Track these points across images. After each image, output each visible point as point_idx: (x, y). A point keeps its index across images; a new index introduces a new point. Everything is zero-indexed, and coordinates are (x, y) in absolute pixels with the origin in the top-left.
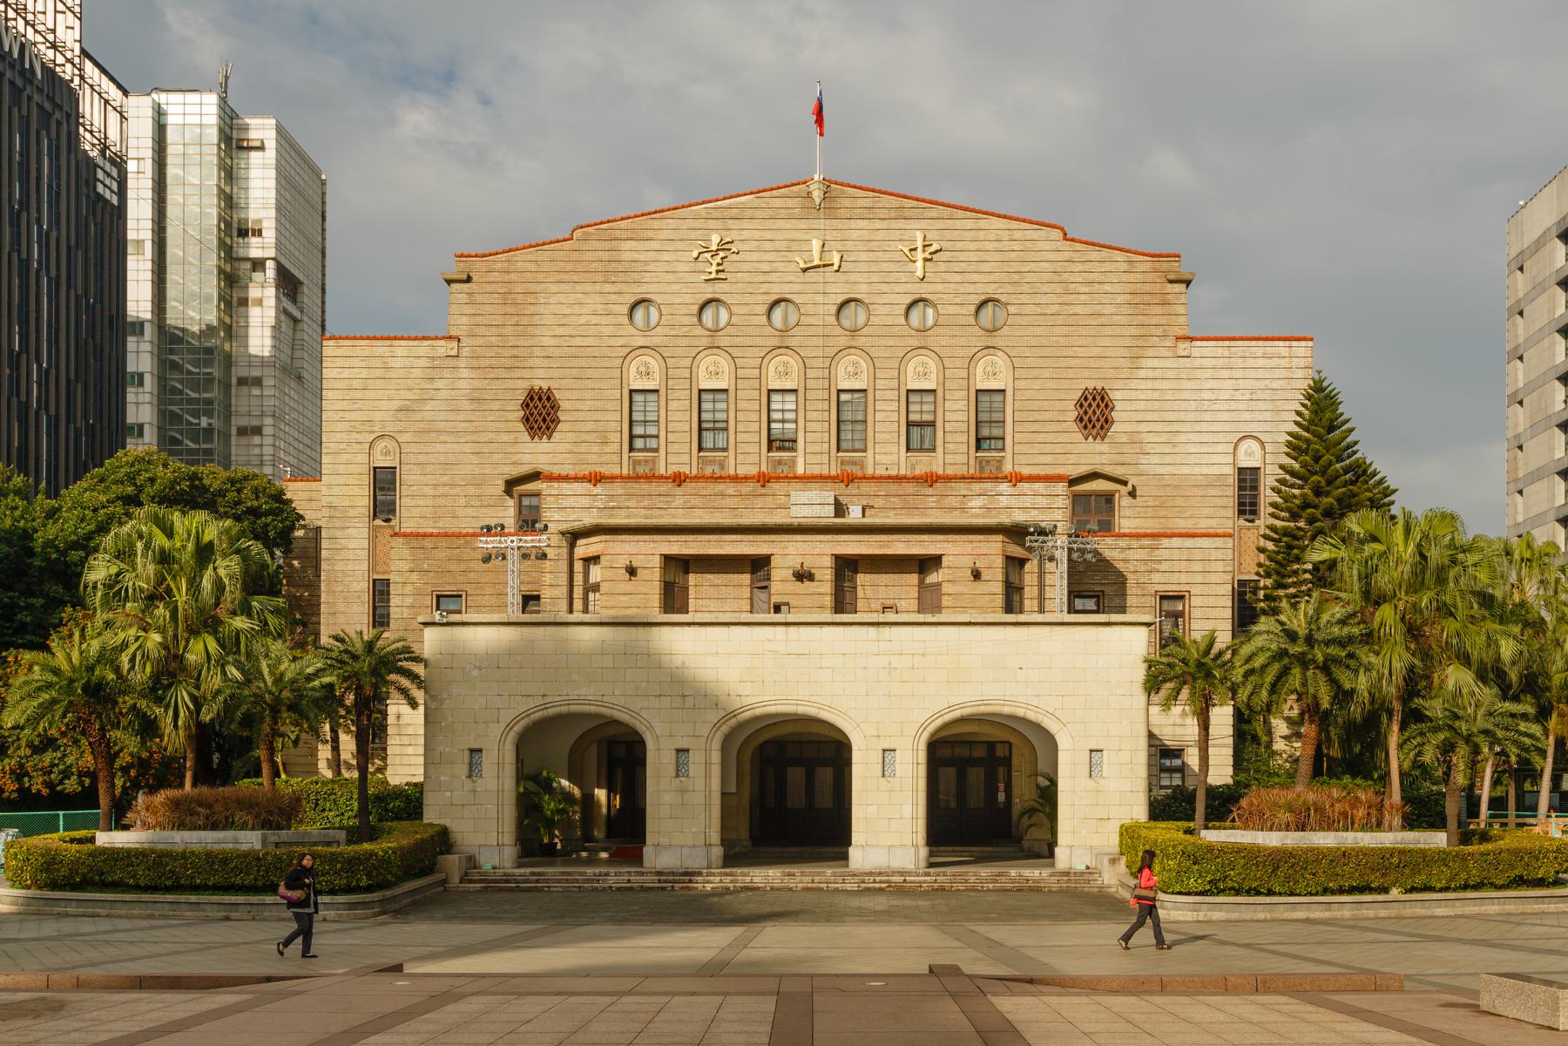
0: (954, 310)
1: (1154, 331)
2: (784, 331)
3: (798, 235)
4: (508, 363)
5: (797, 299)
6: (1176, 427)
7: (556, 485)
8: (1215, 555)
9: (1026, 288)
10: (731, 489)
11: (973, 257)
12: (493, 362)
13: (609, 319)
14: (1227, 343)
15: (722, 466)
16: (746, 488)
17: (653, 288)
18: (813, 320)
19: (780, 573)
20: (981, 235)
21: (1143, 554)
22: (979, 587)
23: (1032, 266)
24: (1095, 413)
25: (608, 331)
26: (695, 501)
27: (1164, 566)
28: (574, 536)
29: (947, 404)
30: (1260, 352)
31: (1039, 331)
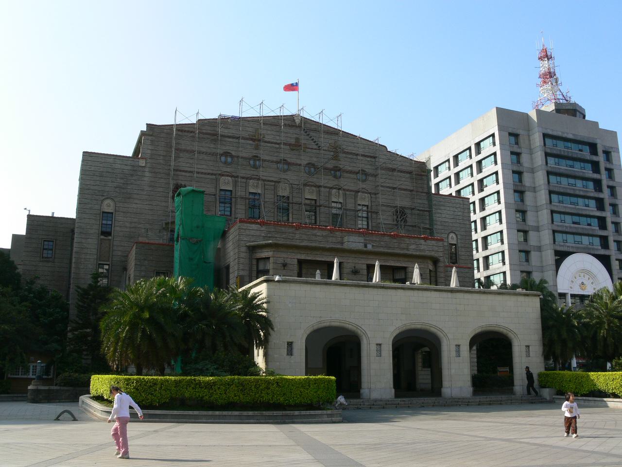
7: (245, 225)
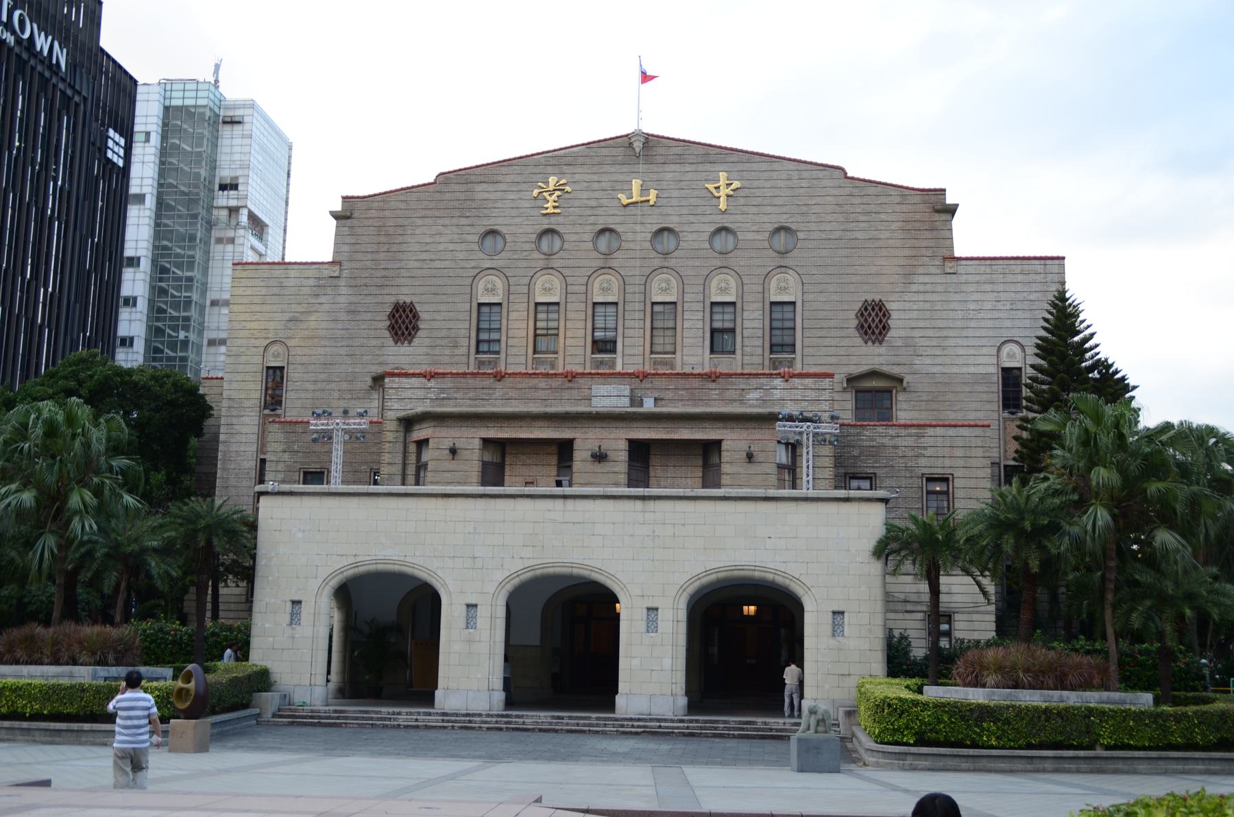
0: (750, 236)
1: (924, 252)
2: (607, 255)
3: (621, 177)
4: (379, 282)
5: (619, 229)
6: (945, 333)
7: (397, 379)
8: (974, 442)
9: (813, 218)
10: (542, 383)
11: (768, 193)
12: (368, 281)
13: (463, 246)
14: (988, 262)
15: (553, 366)
16: (555, 383)
17: (500, 221)
18: (631, 246)
19: (581, 455)
20: (775, 175)
21: (910, 441)
22: (753, 469)
23: (818, 200)
24: (874, 321)
25: (461, 256)
26: (512, 394)
27: (929, 452)
28: (408, 423)
29: (745, 314)
30: (1018, 269)
31: (824, 253)
